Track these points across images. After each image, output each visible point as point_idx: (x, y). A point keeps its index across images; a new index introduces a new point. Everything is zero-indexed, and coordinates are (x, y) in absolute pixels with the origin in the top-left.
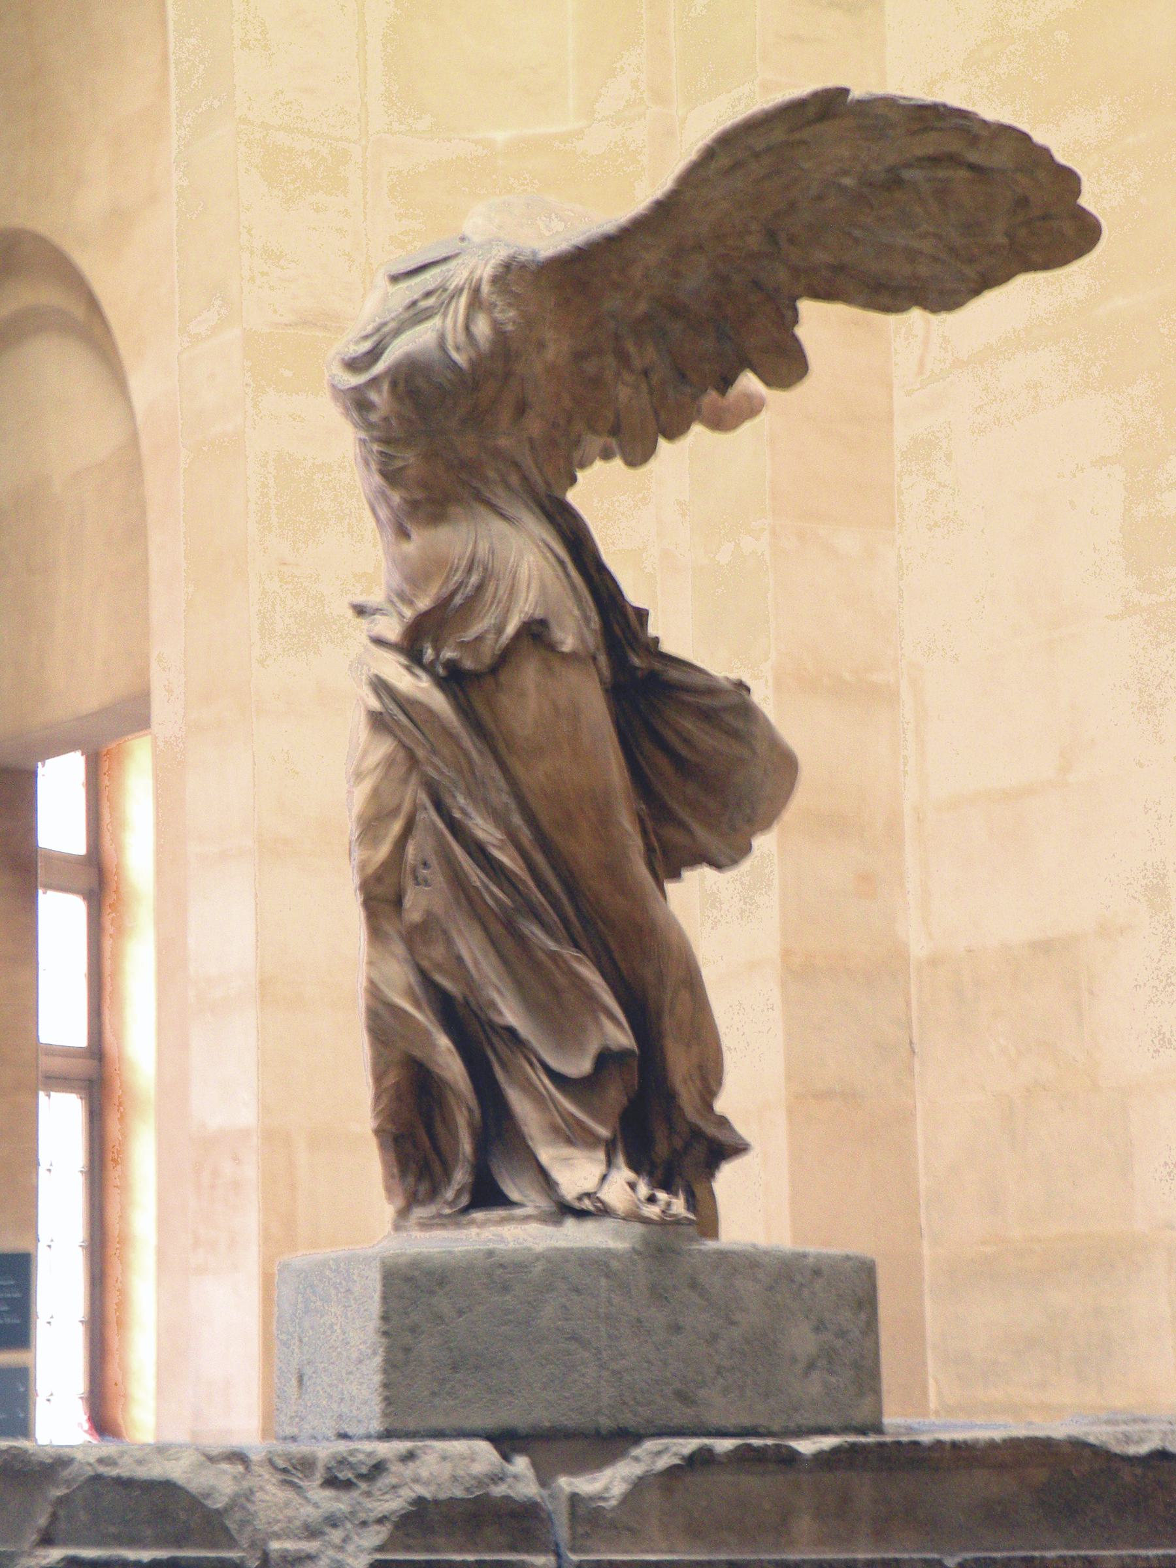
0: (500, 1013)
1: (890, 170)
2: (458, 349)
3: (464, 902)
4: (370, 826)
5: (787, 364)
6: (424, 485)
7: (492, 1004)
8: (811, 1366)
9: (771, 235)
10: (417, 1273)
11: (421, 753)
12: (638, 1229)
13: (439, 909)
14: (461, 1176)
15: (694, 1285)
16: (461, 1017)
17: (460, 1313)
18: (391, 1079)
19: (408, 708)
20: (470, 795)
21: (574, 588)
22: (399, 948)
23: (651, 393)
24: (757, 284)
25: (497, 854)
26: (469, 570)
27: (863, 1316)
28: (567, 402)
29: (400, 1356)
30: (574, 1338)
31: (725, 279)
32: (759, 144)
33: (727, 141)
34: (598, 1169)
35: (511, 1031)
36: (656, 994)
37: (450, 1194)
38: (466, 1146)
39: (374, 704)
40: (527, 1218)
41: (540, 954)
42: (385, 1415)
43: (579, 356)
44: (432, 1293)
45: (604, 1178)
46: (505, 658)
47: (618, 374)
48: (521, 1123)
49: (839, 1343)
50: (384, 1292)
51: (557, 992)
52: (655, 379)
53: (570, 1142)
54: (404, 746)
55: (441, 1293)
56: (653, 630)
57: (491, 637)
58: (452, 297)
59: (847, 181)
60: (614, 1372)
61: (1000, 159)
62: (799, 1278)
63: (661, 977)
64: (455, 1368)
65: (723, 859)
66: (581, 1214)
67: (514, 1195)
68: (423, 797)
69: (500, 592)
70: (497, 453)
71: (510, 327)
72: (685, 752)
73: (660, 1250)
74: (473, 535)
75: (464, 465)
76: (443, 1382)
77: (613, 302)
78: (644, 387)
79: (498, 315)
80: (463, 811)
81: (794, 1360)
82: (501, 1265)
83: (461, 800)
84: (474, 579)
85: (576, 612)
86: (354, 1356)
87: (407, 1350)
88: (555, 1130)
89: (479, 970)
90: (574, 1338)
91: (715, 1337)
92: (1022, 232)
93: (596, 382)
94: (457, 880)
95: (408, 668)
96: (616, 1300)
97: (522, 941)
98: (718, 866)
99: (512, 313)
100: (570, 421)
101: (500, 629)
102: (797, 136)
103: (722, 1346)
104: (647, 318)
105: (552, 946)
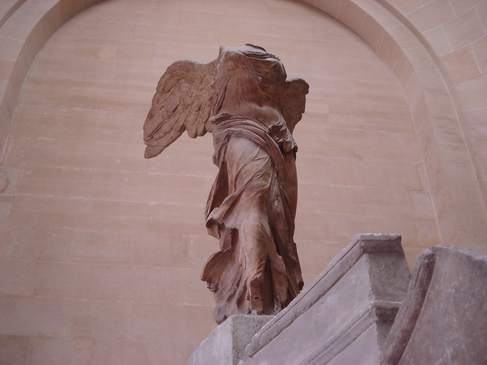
11: (276, 163)
18: (264, 262)
54: (271, 157)
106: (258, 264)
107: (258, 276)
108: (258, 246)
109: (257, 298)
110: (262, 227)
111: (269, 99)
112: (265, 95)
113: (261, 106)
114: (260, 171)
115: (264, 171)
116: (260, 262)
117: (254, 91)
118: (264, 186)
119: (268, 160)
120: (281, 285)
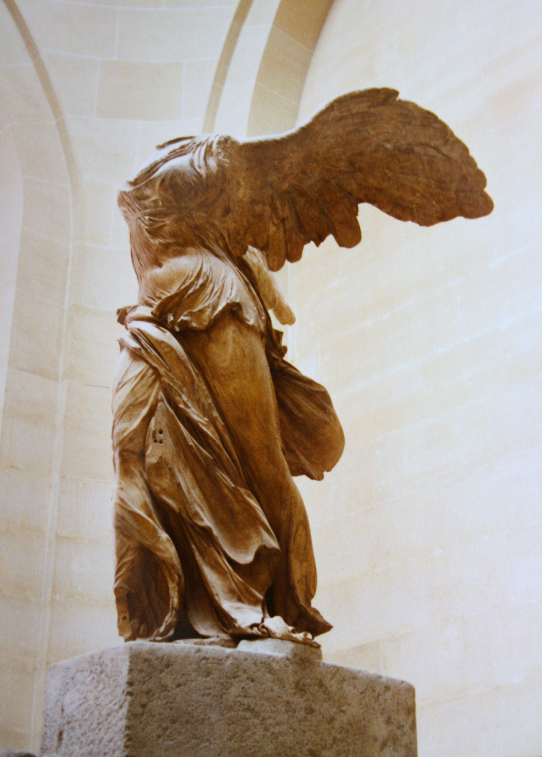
0: (202, 520)
1: (410, 144)
2: (200, 167)
3: (183, 457)
4: (127, 411)
5: (350, 236)
6: (173, 235)
7: (197, 514)
8: (384, 744)
9: (352, 163)
10: (151, 656)
11: (162, 371)
12: (290, 646)
13: (168, 457)
14: (169, 619)
15: (321, 684)
16: (176, 522)
17: (179, 685)
19: (156, 346)
20: (189, 397)
21: (254, 298)
22: (140, 481)
23: (285, 231)
24: (341, 188)
25: (204, 429)
26: (198, 277)
27: (411, 719)
28: (245, 224)
29: (139, 710)
30: (248, 709)
31: (326, 182)
32: (356, 108)
33: (340, 102)
34: (261, 616)
35: (207, 531)
36: (289, 523)
37: (162, 629)
38: (175, 600)
39: (134, 344)
40: (212, 643)
41: (226, 491)
42: (126, 747)
43: (254, 202)
44: (161, 671)
45: (263, 621)
46: (217, 323)
47: (271, 217)
48: (211, 585)
49: (399, 733)
50: (130, 666)
51: (232, 514)
52: (288, 225)
53: (240, 600)
54: (151, 366)
55: (166, 671)
56: (284, 342)
57: (209, 311)
58: (198, 146)
59: (388, 146)
60: (273, 733)
61: (455, 155)
62: (378, 690)
63: (290, 517)
64: (174, 722)
65: (313, 473)
66: (252, 638)
67: (202, 632)
68: (161, 395)
69: (216, 289)
70: (213, 225)
71: (227, 165)
72: (296, 412)
73: (301, 659)
74: (200, 262)
75: (197, 227)
76: (166, 729)
77: (273, 177)
78: (282, 229)
79: (220, 157)
80: (185, 404)
81: (375, 739)
82: (205, 658)
83: (185, 398)
84: (201, 281)
85: (255, 308)
86: (104, 712)
87: (144, 706)
88: (232, 592)
89: (190, 493)
90: (248, 709)
91: (331, 720)
92: (462, 194)
93: (260, 217)
94: (179, 442)
95: (158, 327)
96: (276, 688)
97: (215, 482)
98: (311, 477)
99: (227, 160)
100: (245, 233)
101: (214, 308)
102: (372, 110)
103: (337, 724)
104: (287, 193)
105: (233, 485)
106: (117, 566)
107: (115, 586)
108: (117, 537)
109: (124, 618)
110: (122, 504)
111: (167, 246)
112: (160, 244)
113: (160, 265)
114: (121, 407)
115: (128, 404)
116: (119, 562)
117: (147, 246)
118: (124, 432)
119: (143, 377)
120: (173, 580)
